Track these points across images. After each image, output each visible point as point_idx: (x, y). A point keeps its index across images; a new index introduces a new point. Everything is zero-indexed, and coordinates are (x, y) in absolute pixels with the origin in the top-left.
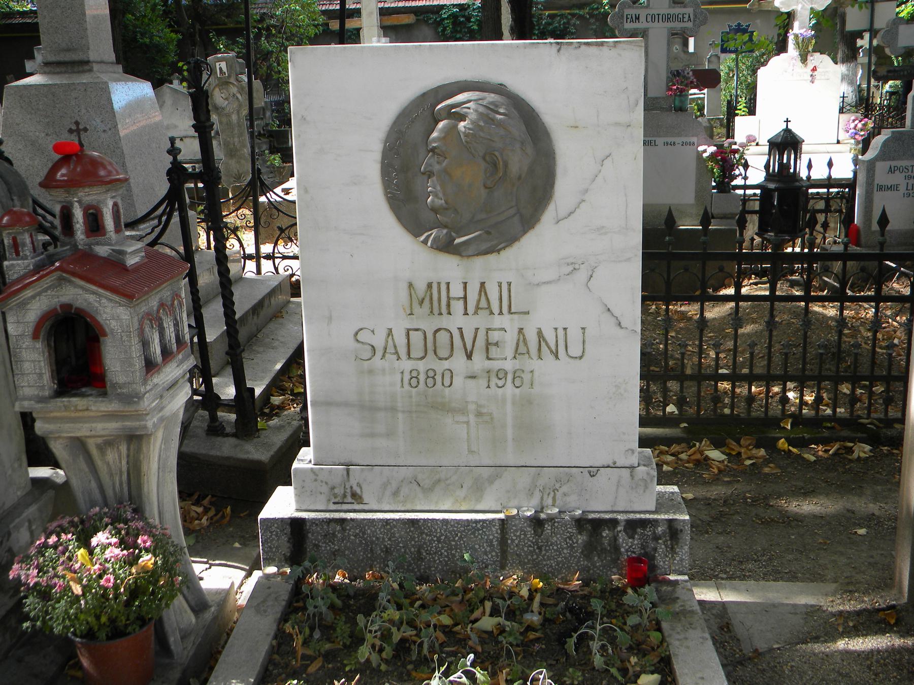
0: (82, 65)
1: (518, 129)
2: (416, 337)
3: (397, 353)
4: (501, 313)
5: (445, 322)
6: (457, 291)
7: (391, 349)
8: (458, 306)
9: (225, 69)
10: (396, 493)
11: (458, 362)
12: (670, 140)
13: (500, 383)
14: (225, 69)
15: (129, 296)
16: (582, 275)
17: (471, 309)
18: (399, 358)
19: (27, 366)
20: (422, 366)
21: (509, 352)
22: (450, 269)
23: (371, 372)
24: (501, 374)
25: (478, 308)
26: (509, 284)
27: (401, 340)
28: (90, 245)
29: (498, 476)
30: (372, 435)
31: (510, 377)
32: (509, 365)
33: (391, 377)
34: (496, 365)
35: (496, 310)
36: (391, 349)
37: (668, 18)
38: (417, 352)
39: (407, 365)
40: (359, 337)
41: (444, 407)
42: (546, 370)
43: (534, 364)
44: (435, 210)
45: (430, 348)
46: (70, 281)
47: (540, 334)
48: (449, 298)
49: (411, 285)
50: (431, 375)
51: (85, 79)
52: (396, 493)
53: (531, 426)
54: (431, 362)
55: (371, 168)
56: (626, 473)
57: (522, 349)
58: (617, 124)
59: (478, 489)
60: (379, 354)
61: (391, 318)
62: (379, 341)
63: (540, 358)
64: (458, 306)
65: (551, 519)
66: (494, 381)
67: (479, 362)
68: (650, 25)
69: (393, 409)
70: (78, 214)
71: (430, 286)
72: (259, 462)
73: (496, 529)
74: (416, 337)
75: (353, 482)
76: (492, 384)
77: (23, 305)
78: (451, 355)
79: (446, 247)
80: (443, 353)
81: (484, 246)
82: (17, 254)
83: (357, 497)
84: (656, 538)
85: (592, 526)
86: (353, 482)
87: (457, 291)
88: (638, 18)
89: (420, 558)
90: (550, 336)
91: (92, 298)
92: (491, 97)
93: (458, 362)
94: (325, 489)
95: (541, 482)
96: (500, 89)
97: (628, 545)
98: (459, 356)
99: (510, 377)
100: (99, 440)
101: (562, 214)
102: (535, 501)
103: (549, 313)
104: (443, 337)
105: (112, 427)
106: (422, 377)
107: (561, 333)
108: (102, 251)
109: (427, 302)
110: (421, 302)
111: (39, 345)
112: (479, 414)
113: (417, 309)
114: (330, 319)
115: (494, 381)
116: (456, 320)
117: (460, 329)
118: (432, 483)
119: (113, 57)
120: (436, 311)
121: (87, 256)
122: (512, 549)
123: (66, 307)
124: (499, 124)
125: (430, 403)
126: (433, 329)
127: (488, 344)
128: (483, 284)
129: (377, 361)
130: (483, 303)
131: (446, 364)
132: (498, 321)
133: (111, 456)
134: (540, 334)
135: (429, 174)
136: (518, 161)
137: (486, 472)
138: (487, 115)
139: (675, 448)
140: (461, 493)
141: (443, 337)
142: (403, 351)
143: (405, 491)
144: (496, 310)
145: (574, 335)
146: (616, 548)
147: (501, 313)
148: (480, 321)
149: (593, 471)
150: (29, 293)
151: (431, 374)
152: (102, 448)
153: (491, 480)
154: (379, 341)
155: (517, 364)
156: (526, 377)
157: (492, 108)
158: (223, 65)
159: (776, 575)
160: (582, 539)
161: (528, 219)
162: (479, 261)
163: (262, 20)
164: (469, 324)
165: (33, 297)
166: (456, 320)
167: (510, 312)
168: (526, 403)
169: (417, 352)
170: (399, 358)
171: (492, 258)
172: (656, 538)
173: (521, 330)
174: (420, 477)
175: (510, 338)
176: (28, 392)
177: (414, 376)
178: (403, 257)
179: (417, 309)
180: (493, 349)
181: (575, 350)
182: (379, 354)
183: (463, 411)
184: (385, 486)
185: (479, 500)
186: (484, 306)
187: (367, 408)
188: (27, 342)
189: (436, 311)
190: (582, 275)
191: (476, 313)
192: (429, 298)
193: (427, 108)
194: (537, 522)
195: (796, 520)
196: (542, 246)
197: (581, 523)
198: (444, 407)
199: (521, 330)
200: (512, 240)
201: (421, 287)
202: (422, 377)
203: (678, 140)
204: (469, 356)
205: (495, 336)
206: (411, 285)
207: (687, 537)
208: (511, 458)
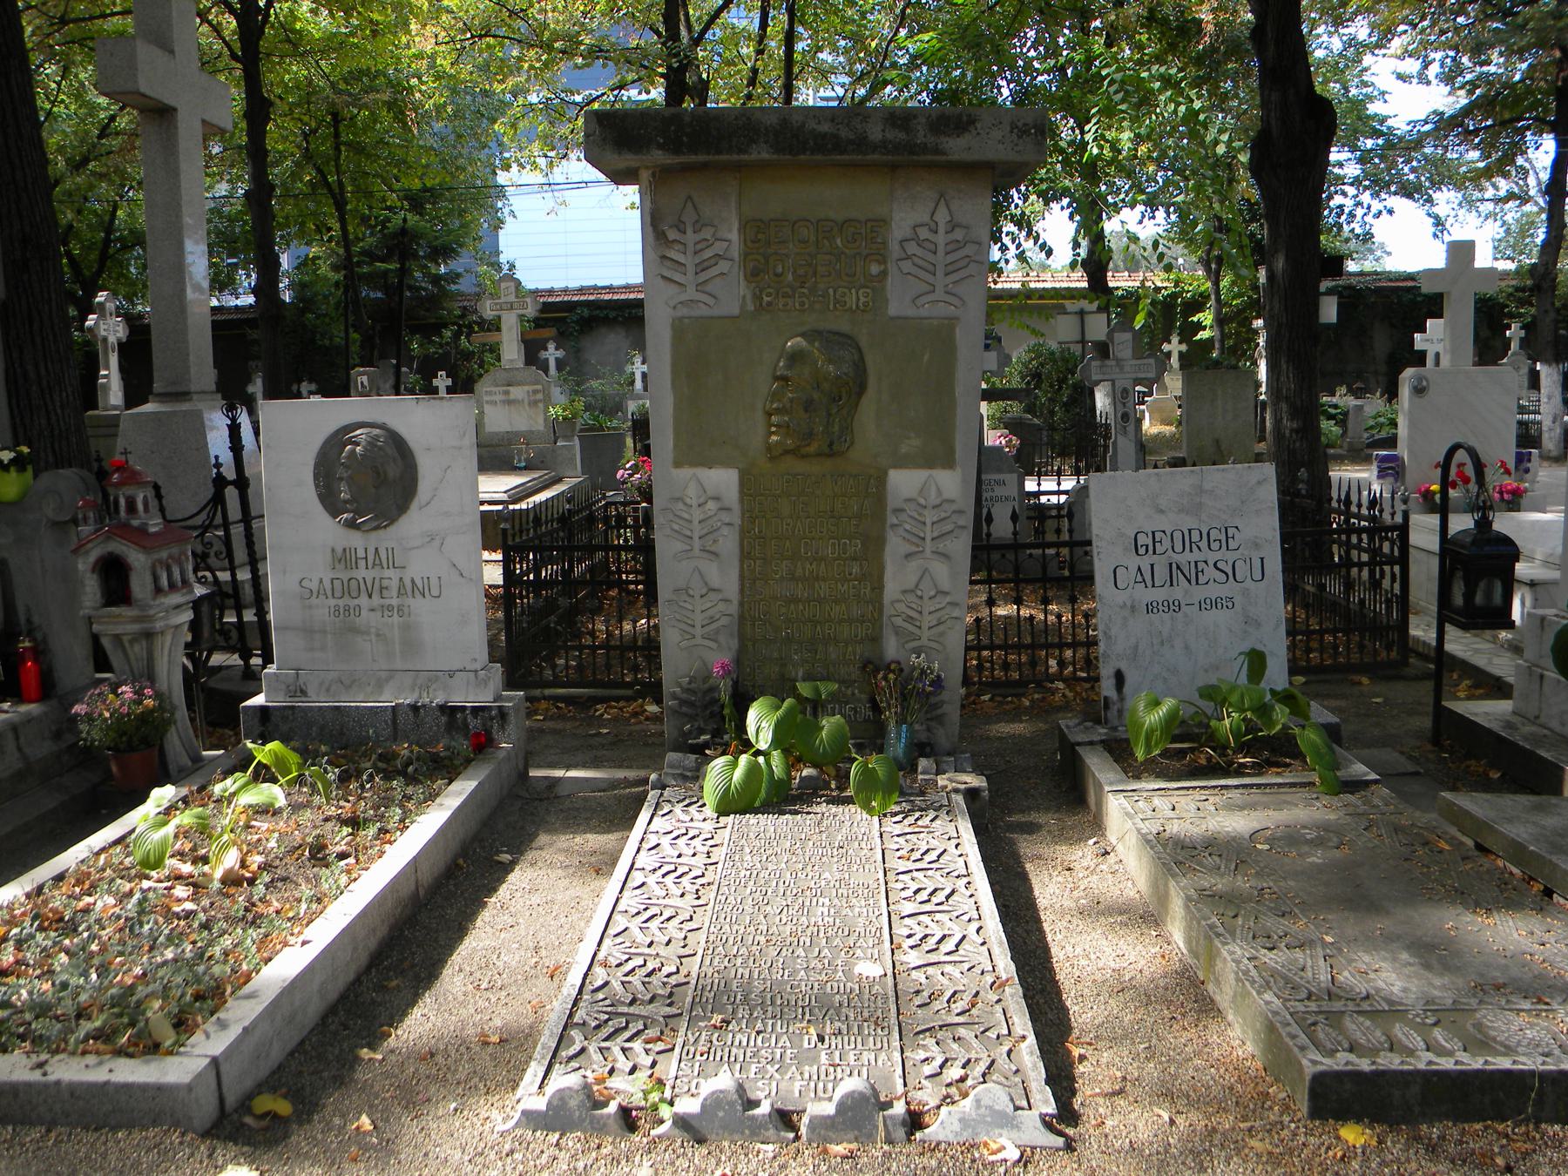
0: (183, 396)
1: (391, 451)
5: (354, 574)
6: (361, 554)
8: (362, 563)
10: (328, 690)
11: (363, 600)
15: (145, 549)
16: (437, 543)
19: (88, 589)
20: (341, 603)
21: (395, 594)
22: (356, 540)
23: (310, 607)
24: (390, 608)
29: (391, 677)
30: (312, 649)
32: (394, 602)
33: (322, 611)
34: (387, 602)
38: (338, 594)
39: (332, 602)
41: (355, 630)
42: (418, 605)
43: (410, 601)
44: (346, 502)
45: (347, 591)
50: (347, 609)
51: (185, 407)
52: (328, 690)
53: (411, 644)
54: (346, 600)
56: (472, 675)
59: (380, 686)
61: (321, 572)
62: (314, 585)
64: (362, 563)
65: (424, 706)
67: (376, 598)
69: (324, 632)
70: (122, 502)
73: (389, 712)
75: (301, 682)
77: (87, 553)
79: (351, 524)
80: (354, 594)
81: (375, 524)
83: (304, 693)
84: (492, 719)
85: (448, 711)
86: (301, 682)
87: (361, 554)
89: (342, 734)
92: (376, 431)
93: (363, 600)
95: (419, 682)
96: (382, 427)
97: (474, 724)
102: (416, 695)
105: (135, 627)
108: (135, 523)
112: (378, 635)
116: (361, 573)
118: (349, 683)
119: (214, 387)
121: (126, 525)
122: (401, 726)
123: (111, 554)
124: (380, 448)
125: (347, 629)
126: (348, 579)
127: (381, 588)
129: (314, 600)
131: (356, 602)
132: (387, 573)
133: (137, 648)
135: (341, 479)
136: (393, 471)
138: (373, 442)
139: (622, 704)
140: (369, 689)
142: (329, 593)
143: (333, 688)
145: (434, 581)
146: (466, 725)
153: (387, 680)
154: (314, 585)
157: (376, 438)
158: (365, 379)
159: (620, 767)
160: (444, 719)
162: (374, 535)
163: (463, 316)
164: (369, 575)
166: (361, 573)
168: (406, 628)
169: (338, 594)
171: (381, 532)
172: (492, 719)
175: (394, 584)
176: (88, 604)
178: (327, 531)
181: (435, 592)
183: (368, 633)
184: (321, 684)
185: (381, 694)
187: (308, 631)
188: (89, 575)
190: (437, 543)
192: (344, 559)
193: (340, 438)
194: (415, 708)
196: (413, 524)
197: (443, 708)
198: (355, 630)
200: (393, 521)
201: (339, 551)
205: (385, 583)
207: (512, 718)
208: (399, 665)
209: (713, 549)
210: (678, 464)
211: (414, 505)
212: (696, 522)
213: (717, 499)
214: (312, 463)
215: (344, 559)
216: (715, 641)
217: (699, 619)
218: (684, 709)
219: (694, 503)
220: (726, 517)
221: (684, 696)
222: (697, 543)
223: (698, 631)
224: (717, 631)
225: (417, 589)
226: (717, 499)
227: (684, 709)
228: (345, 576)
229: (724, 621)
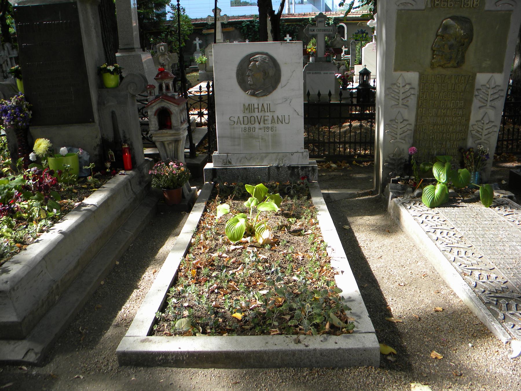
0: (132, 49)
2: (246, 119)
5: (253, 114)
6: (256, 106)
7: (239, 122)
8: (256, 110)
9: (163, 49)
10: (240, 161)
11: (257, 125)
12: (325, 72)
14: (163, 49)
15: (178, 104)
16: (288, 101)
17: (260, 111)
20: (247, 126)
21: (270, 122)
22: (254, 101)
23: (234, 128)
24: (268, 128)
25: (261, 110)
27: (241, 119)
30: (234, 145)
32: (270, 126)
33: (239, 129)
34: (266, 126)
35: (266, 111)
36: (239, 122)
37: (324, 30)
38: (246, 122)
39: (243, 126)
41: (252, 137)
42: (280, 127)
43: (276, 125)
44: (250, 85)
45: (249, 122)
47: (278, 117)
49: (244, 105)
50: (249, 129)
51: (133, 53)
52: (240, 161)
53: (276, 142)
54: (249, 125)
56: (301, 154)
57: (273, 121)
58: (296, 63)
59: (262, 159)
62: (236, 120)
64: (256, 110)
66: (266, 130)
67: (262, 125)
68: (318, 33)
69: (239, 138)
70: (164, 85)
71: (249, 105)
72: (198, 164)
74: (246, 119)
75: (229, 158)
77: (152, 107)
79: (253, 94)
80: (253, 123)
81: (263, 94)
83: (230, 163)
84: (309, 171)
85: (292, 168)
86: (229, 158)
87: (256, 106)
88: (314, 30)
91: (169, 105)
92: (264, 56)
93: (257, 125)
94: (221, 161)
96: (267, 54)
98: (257, 123)
103: (279, 112)
104: (253, 118)
105: (172, 138)
108: (169, 94)
110: (247, 109)
111: (156, 117)
112: (262, 139)
113: (246, 111)
114: (223, 114)
115: (266, 130)
116: (256, 114)
118: (250, 158)
119: (140, 46)
123: (163, 107)
124: (267, 63)
127: (264, 120)
129: (235, 125)
130: (263, 109)
131: (253, 126)
132: (267, 114)
133: (170, 146)
134: (278, 117)
135: (249, 76)
136: (271, 72)
137: (264, 155)
138: (263, 61)
140: (258, 161)
141: (253, 118)
142: (242, 122)
144: (266, 111)
145: (287, 117)
149: (292, 154)
150: (154, 104)
152: (168, 144)
153: (266, 157)
154: (236, 120)
156: (274, 129)
157: (265, 59)
158: (163, 47)
159: (345, 188)
160: (289, 172)
161: (274, 87)
162: (262, 98)
163: (168, 29)
164: (259, 115)
166: (256, 114)
169: (246, 122)
171: (265, 97)
172: (309, 171)
175: (270, 118)
176: (152, 129)
178: (242, 97)
179: (246, 111)
181: (287, 121)
182: (236, 123)
183: (258, 138)
184: (237, 159)
185: (262, 162)
186: (263, 110)
187: (232, 138)
190: (288, 101)
192: (249, 108)
193: (248, 59)
194: (278, 168)
195: (355, 179)
196: (278, 94)
198: (252, 137)
200: (270, 92)
201: (247, 105)
203: (329, 72)
204: (259, 124)
205: (266, 118)
206: (244, 105)
208: (271, 151)
209: (406, 104)
210: (395, 70)
211: (279, 86)
212: (401, 93)
213: (409, 84)
216: (405, 140)
217: (399, 131)
218: (390, 167)
219: (401, 86)
220: (412, 92)
221: (391, 161)
222: (401, 101)
223: (398, 136)
224: (405, 137)
225: (280, 120)
226: (409, 84)
227: (390, 167)
228: (249, 115)
229: (409, 132)
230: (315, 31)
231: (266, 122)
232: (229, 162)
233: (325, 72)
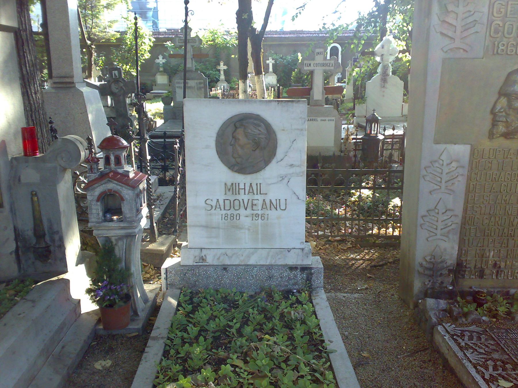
2: (227, 202)
3: (220, 208)
4: (257, 194)
7: (218, 206)
11: (242, 211)
12: (323, 118)
13: (257, 219)
16: (286, 180)
17: (247, 192)
18: (221, 210)
19: (94, 211)
20: (229, 212)
21: (260, 207)
24: (257, 215)
25: (249, 192)
26: (260, 184)
28: (116, 169)
31: (260, 216)
32: (260, 212)
34: (255, 212)
35: (255, 193)
37: (323, 65)
38: (227, 207)
39: (224, 212)
40: (207, 202)
42: (273, 214)
43: (269, 212)
45: (232, 206)
46: (111, 182)
47: (271, 201)
48: (239, 188)
49: (226, 184)
50: (232, 216)
54: (232, 211)
55: (212, 143)
57: (264, 207)
58: (298, 129)
60: (214, 208)
62: (214, 203)
63: (271, 210)
66: (254, 218)
69: (219, 228)
70: (112, 158)
71: (232, 184)
74: (227, 202)
76: (254, 219)
78: (240, 208)
80: (236, 208)
82: (92, 172)
87: (242, 186)
88: (310, 65)
90: (274, 202)
93: (242, 211)
98: (242, 209)
99: (260, 216)
100: (116, 238)
101: (279, 160)
103: (275, 193)
104: (237, 202)
105: (122, 232)
106: (229, 216)
107: (278, 201)
109: (231, 189)
110: (229, 190)
114: (196, 195)
115: (254, 218)
117: (243, 200)
120: (234, 193)
121: (116, 173)
127: (253, 205)
128: (251, 184)
129: (213, 211)
130: (251, 191)
131: (238, 212)
132: (256, 197)
134: (271, 201)
137: (252, 250)
141: (237, 202)
144: (255, 193)
145: (283, 202)
147: (257, 194)
148: (251, 196)
149: (289, 250)
151: (232, 215)
153: (253, 254)
155: (263, 212)
156: (266, 216)
161: (267, 162)
165: (98, 187)
167: (260, 194)
169: (227, 207)
170: (221, 210)
173: (264, 200)
174: (228, 253)
175: (260, 203)
176: (93, 220)
177: (226, 216)
178: (223, 174)
180: (254, 207)
181: (283, 207)
182: (214, 208)
186: (251, 191)
188: (94, 203)
189: (234, 193)
190: (286, 180)
191: (248, 194)
196: (272, 171)
199: (264, 200)
201: (229, 184)
202: (229, 216)
203: (327, 119)
204: (246, 209)
205: (255, 202)
209: (451, 188)
210: (437, 142)
211: (274, 161)
212: (444, 173)
213: (457, 161)
214: (215, 135)
215: (232, 189)
216: (447, 237)
217: (440, 225)
218: (427, 272)
219: (445, 164)
220: (461, 171)
221: (427, 266)
222: (443, 185)
223: (439, 232)
224: (448, 232)
225: (274, 206)
226: (457, 161)
227: (427, 272)
229: (453, 226)
230: (312, 65)
231: (254, 208)
232: (203, 260)
233: (323, 118)
